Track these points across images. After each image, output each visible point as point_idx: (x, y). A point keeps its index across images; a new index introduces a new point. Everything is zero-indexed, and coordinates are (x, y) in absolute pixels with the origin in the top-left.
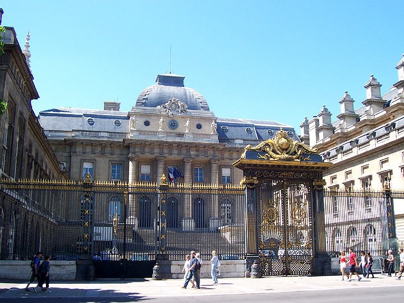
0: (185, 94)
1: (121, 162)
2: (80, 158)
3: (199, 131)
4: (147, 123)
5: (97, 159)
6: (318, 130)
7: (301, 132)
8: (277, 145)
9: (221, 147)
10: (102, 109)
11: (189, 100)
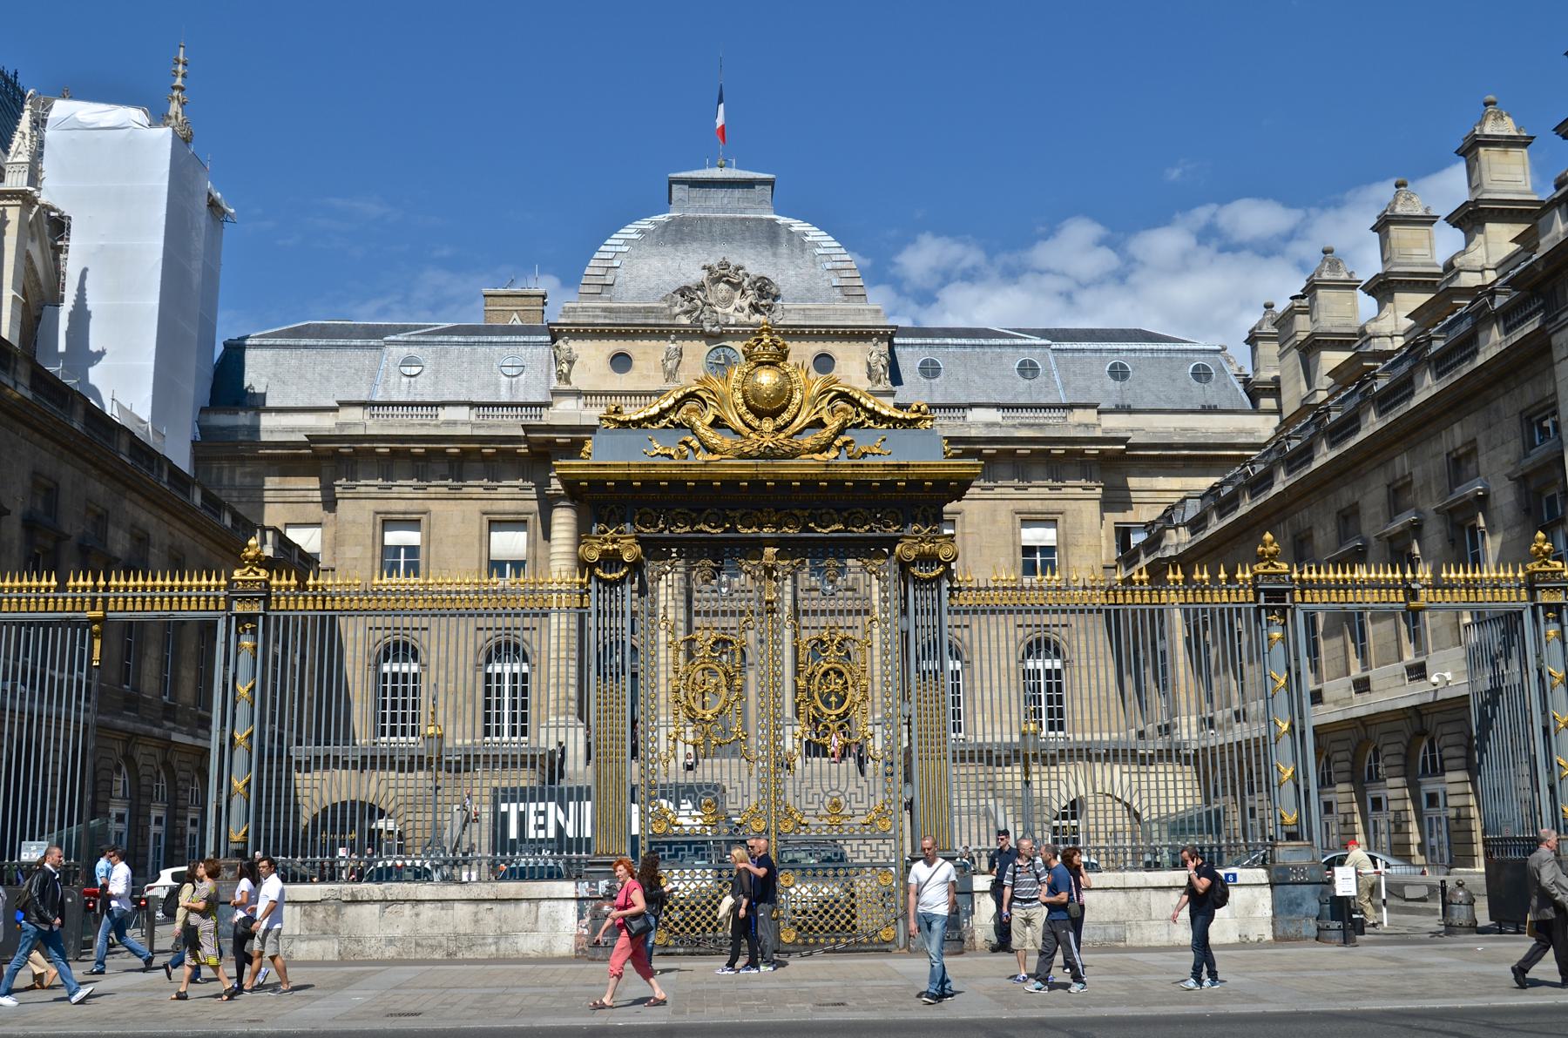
1: (523, 517)
2: (372, 505)
4: (621, 362)
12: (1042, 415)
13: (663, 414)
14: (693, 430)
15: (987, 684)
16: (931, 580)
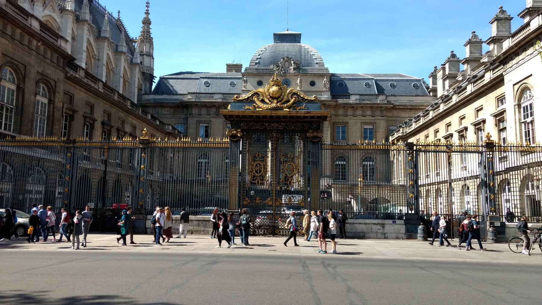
0: (300, 51)
2: (196, 119)
3: (313, 89)
5: (212, 120)
6: (445, 78)
8: (267, 94)
9: (333, 103)
10: (225, 71)
11: (303, 57)
12: (370, 97)
13: (248, 98)
14: (255, 102)
15: (354, 168)
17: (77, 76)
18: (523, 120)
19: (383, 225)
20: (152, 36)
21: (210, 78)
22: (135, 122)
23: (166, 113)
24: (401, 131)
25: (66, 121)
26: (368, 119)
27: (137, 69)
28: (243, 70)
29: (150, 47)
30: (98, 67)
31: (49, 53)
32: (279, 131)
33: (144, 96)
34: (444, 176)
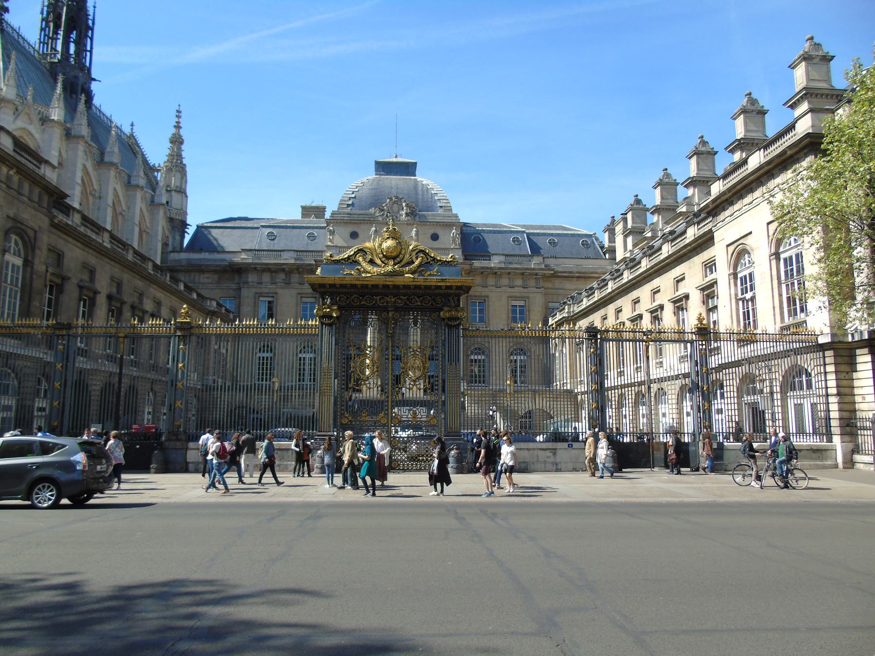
2: (254, 290)
3: (436, 244)
5: (279, 291)
6: (626, 234)
7: (605, 239)
8: (379, 251)
9: (467, 267)
11: (420, 197)
12: (520, 259)
13: (349, 258)
14: (359, 264)
16: (455, 326)
17: (70, 223)
18: (740, 296)
19: (554, 451)
20: (185, 161)
21: (277, 227)
22: (160, 294)
23: (206, 280)
24: (566, 310)
25: (51, 293)
26: (517, 291)
27: (161, 213)
28: (328, 215)
29: (182, 178)
30: (99, 209)
31: (26, 186)
32: (397, 309)
33: (172, 254)
34: (641, 376)
